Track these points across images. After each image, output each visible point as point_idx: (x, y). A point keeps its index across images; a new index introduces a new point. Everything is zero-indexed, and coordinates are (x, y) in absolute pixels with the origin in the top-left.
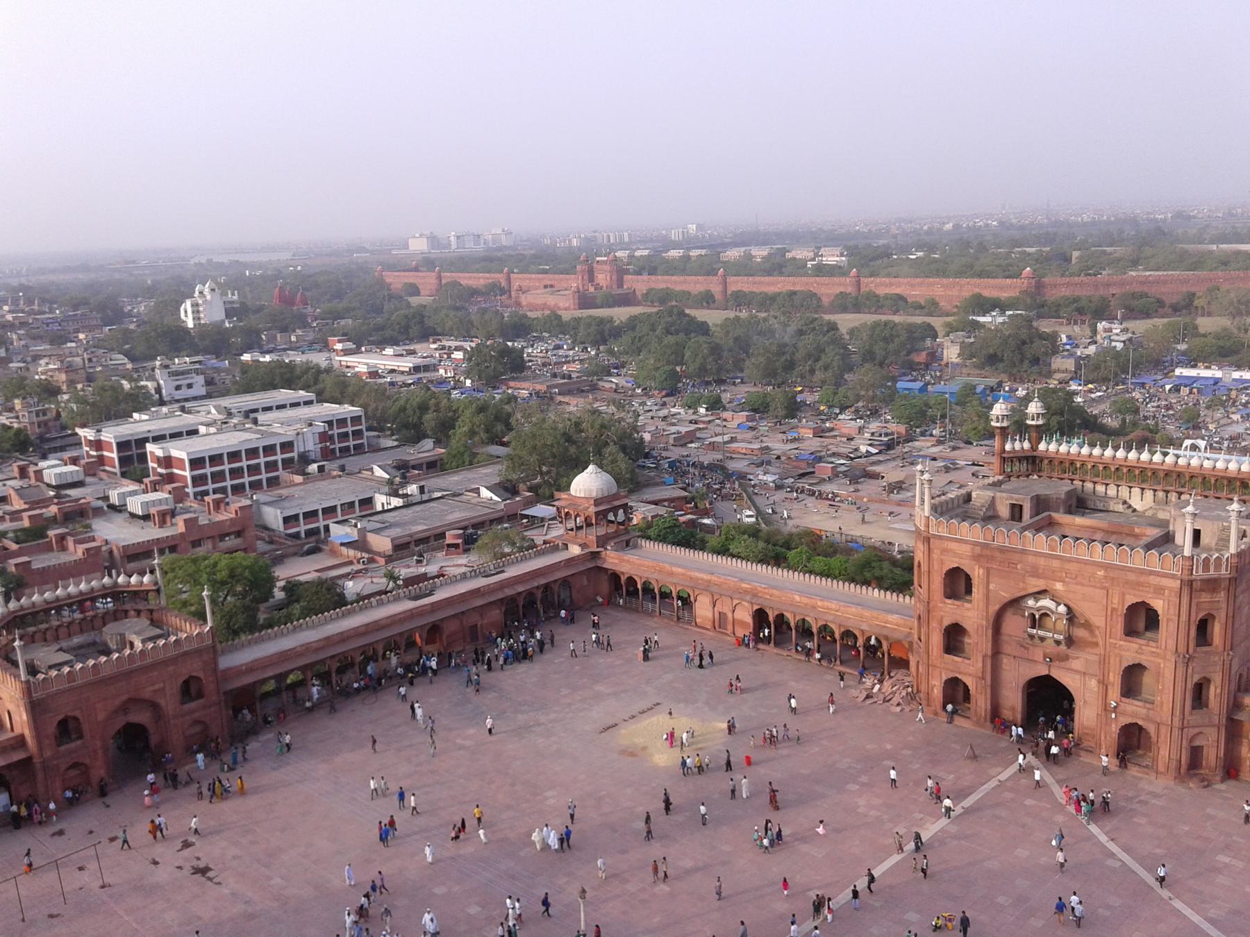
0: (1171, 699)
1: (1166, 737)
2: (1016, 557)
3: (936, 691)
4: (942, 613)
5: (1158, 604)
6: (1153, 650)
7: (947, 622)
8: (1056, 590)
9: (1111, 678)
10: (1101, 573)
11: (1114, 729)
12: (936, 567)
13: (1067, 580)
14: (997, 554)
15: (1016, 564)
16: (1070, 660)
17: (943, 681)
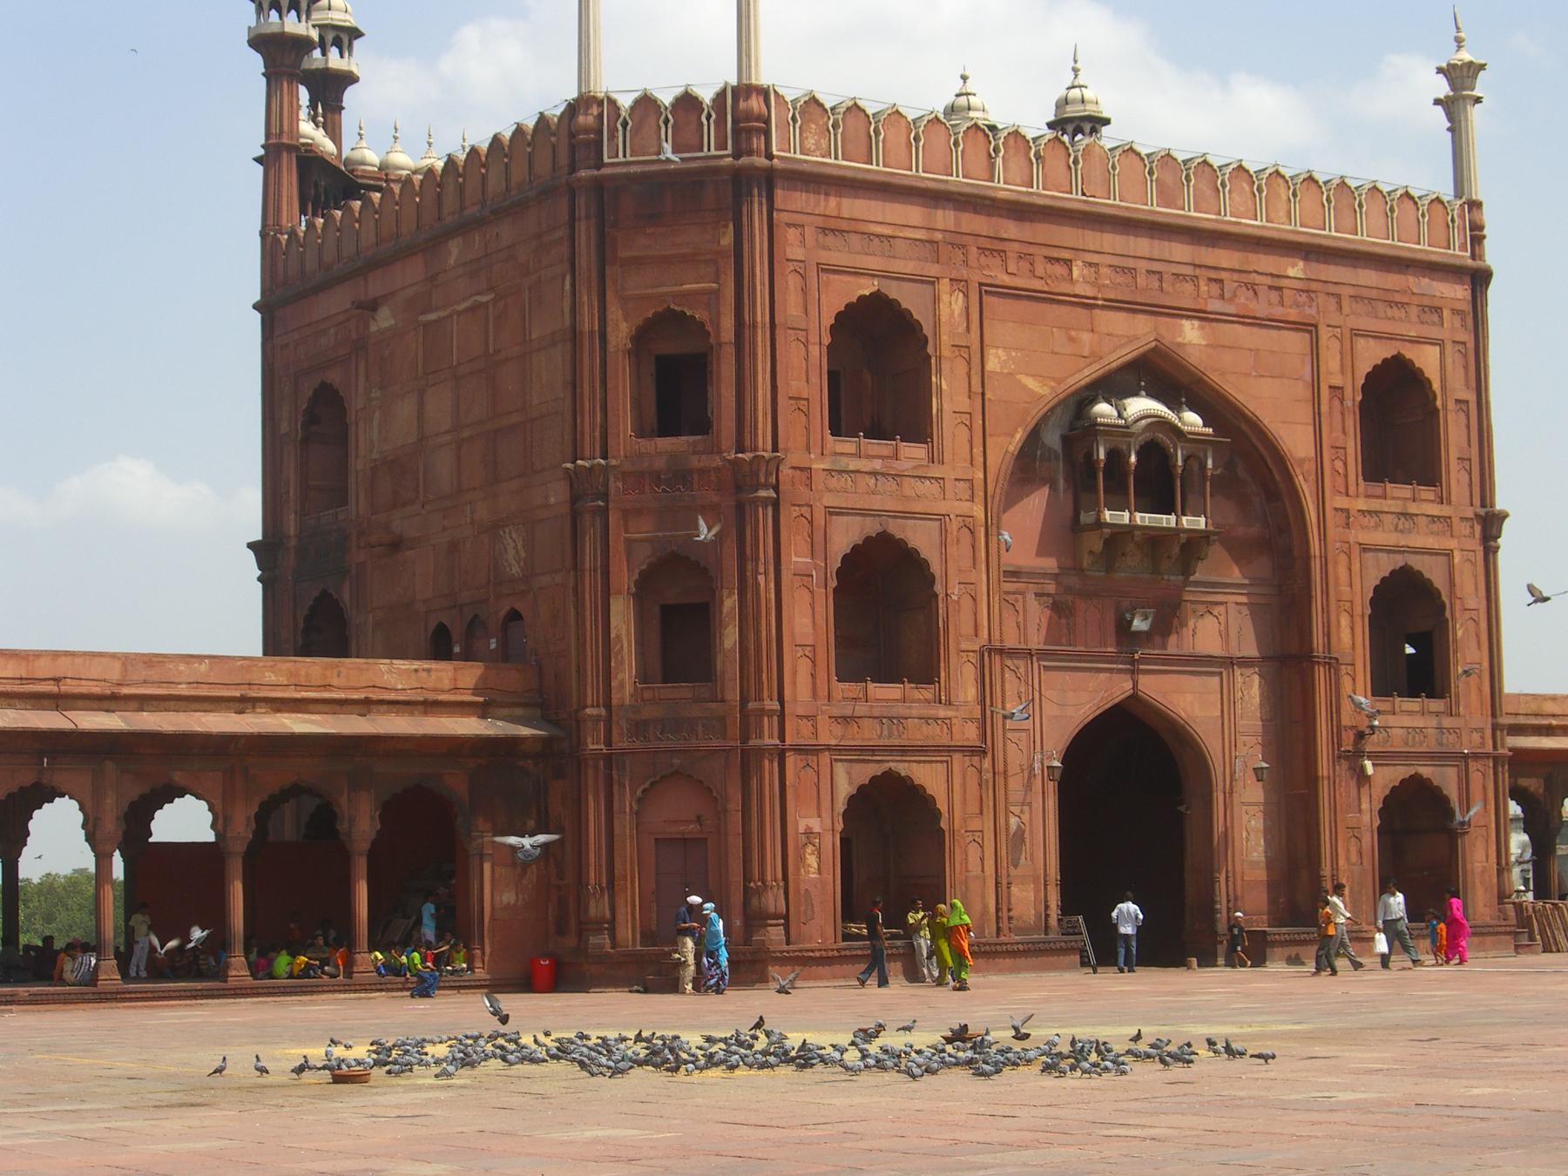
0: (1486, 664)
1: (1485, 800)
2: (1067, 235)
3: (812, 860)
4: (830, 500)
5: (1427, 360)
6: (1434, 510)
7: (845, 536)
8: (1179, 345)
9: (1345, 636)
10: (1296, 269)
11: (1366, 818)
12: (791, 306)
13: (1215, 305)
14: (1010, 229)
15: (1068, 263)
16: (1191, 623)
17: (841, 806)
